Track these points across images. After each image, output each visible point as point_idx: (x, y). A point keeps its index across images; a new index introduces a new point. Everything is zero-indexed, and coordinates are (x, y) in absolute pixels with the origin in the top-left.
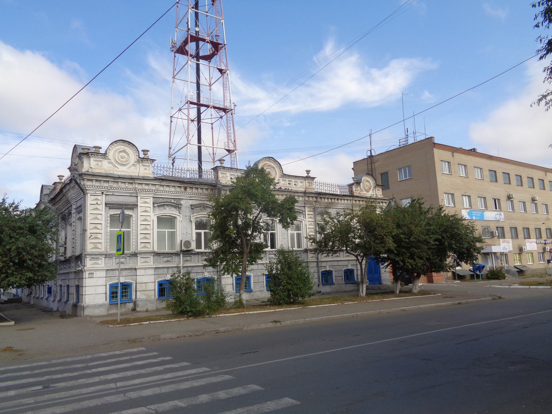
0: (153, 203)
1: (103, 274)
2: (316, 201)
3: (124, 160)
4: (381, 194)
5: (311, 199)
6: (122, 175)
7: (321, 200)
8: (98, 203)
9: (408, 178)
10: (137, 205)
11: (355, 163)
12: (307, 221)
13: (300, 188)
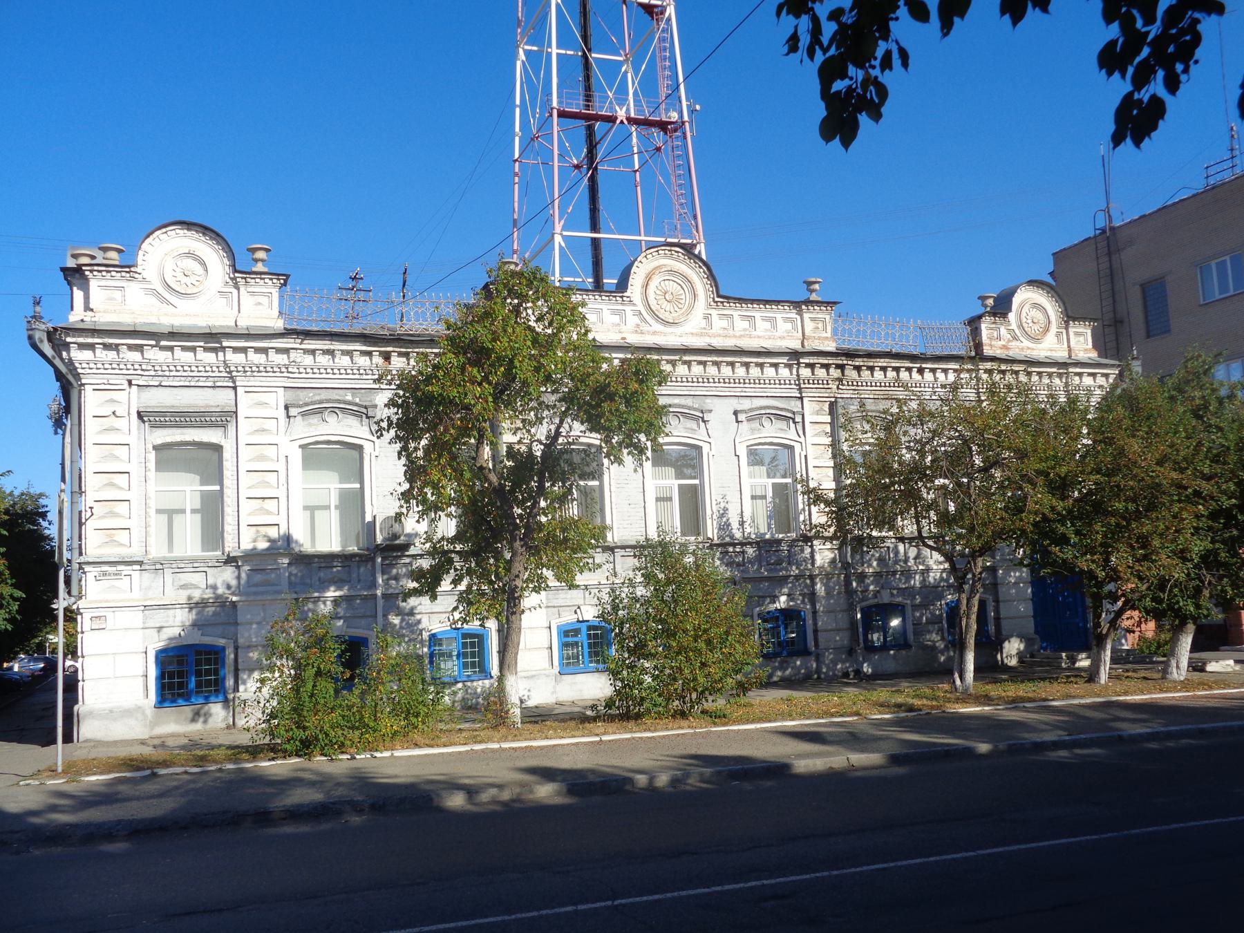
0: (286, 408)
1: (136, 618)
2: (840, 380)
3: (193, 279)
4: (1090, 345)
5: (821, 373)
6: (181, 327)
7: (860, 376)
8: (117, 414)
9: (1232, 292)
10: (236, 413)
11: (1059, 257)
12: (809, 446)
13: (782, 338)
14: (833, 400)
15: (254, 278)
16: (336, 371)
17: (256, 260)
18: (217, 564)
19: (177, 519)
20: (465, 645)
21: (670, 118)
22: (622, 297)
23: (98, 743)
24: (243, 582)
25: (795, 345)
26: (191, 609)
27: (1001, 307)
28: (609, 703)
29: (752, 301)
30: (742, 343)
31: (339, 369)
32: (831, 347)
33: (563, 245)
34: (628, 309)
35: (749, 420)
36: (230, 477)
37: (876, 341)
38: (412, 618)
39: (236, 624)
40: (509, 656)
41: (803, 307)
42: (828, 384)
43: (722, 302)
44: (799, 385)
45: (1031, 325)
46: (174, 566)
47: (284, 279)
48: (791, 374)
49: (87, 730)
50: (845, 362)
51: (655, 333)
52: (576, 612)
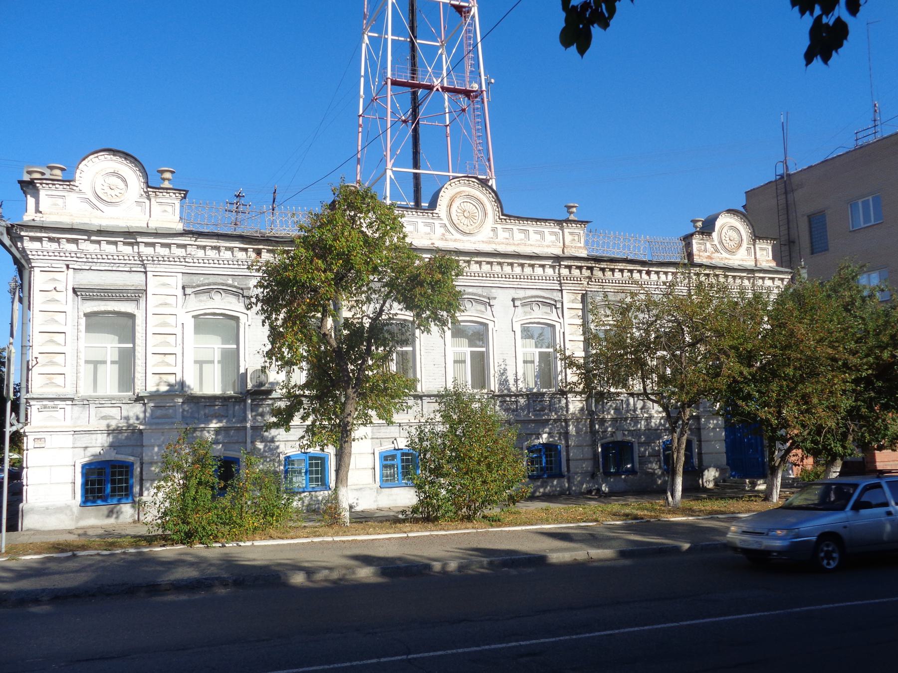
0: (184, 288)
1: (68, 440)
2: (590, 278)
3: (117, 192)
4: (771, 257)
5: (576, 272)
6: (107, 226)
7: (604, 275)
8: (57, 289)
9: (873, 223)
10: (146, 291)
12: (566, 325)
13: (548, 246)
14: (584, 292)
15: (162, 192)
16: (221, 262)
17: (164, 179)
18: (129, 402)
19: (100, 367)
20: (311, 465)
21: (472, 87)
22: (432, 213)
23: (37, 532)
24: (148, 415)
25: (558, 251)
26: (109, 434)
27: (707, 228)
28: (415, 510)
29: (527, 219)
30: (519, 249)
31: (223, 261)
32: (584, 254)
33: (393, 177)
34: (437, 222)
35: (523, 305)
36: (141, 338)
37: (616, 250)
38: (273, 444)
39: (142, 446)
40: (342, 473)
41: (564, 224)
42: (581, 281)
43: (505, 219)
44: (560, 281)
45: (728, 241)
46: (97, 402)
47: (185, 194)
48: (555, 273)
49: (28, 522)
50: (594, 265)
51: (455, 240)
52: (393, 443)
